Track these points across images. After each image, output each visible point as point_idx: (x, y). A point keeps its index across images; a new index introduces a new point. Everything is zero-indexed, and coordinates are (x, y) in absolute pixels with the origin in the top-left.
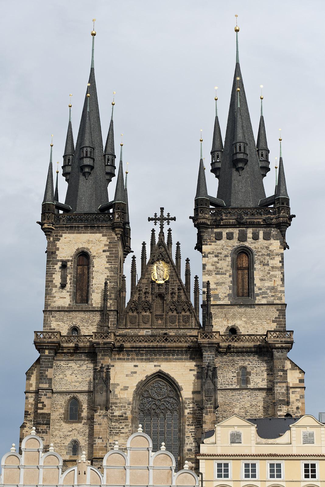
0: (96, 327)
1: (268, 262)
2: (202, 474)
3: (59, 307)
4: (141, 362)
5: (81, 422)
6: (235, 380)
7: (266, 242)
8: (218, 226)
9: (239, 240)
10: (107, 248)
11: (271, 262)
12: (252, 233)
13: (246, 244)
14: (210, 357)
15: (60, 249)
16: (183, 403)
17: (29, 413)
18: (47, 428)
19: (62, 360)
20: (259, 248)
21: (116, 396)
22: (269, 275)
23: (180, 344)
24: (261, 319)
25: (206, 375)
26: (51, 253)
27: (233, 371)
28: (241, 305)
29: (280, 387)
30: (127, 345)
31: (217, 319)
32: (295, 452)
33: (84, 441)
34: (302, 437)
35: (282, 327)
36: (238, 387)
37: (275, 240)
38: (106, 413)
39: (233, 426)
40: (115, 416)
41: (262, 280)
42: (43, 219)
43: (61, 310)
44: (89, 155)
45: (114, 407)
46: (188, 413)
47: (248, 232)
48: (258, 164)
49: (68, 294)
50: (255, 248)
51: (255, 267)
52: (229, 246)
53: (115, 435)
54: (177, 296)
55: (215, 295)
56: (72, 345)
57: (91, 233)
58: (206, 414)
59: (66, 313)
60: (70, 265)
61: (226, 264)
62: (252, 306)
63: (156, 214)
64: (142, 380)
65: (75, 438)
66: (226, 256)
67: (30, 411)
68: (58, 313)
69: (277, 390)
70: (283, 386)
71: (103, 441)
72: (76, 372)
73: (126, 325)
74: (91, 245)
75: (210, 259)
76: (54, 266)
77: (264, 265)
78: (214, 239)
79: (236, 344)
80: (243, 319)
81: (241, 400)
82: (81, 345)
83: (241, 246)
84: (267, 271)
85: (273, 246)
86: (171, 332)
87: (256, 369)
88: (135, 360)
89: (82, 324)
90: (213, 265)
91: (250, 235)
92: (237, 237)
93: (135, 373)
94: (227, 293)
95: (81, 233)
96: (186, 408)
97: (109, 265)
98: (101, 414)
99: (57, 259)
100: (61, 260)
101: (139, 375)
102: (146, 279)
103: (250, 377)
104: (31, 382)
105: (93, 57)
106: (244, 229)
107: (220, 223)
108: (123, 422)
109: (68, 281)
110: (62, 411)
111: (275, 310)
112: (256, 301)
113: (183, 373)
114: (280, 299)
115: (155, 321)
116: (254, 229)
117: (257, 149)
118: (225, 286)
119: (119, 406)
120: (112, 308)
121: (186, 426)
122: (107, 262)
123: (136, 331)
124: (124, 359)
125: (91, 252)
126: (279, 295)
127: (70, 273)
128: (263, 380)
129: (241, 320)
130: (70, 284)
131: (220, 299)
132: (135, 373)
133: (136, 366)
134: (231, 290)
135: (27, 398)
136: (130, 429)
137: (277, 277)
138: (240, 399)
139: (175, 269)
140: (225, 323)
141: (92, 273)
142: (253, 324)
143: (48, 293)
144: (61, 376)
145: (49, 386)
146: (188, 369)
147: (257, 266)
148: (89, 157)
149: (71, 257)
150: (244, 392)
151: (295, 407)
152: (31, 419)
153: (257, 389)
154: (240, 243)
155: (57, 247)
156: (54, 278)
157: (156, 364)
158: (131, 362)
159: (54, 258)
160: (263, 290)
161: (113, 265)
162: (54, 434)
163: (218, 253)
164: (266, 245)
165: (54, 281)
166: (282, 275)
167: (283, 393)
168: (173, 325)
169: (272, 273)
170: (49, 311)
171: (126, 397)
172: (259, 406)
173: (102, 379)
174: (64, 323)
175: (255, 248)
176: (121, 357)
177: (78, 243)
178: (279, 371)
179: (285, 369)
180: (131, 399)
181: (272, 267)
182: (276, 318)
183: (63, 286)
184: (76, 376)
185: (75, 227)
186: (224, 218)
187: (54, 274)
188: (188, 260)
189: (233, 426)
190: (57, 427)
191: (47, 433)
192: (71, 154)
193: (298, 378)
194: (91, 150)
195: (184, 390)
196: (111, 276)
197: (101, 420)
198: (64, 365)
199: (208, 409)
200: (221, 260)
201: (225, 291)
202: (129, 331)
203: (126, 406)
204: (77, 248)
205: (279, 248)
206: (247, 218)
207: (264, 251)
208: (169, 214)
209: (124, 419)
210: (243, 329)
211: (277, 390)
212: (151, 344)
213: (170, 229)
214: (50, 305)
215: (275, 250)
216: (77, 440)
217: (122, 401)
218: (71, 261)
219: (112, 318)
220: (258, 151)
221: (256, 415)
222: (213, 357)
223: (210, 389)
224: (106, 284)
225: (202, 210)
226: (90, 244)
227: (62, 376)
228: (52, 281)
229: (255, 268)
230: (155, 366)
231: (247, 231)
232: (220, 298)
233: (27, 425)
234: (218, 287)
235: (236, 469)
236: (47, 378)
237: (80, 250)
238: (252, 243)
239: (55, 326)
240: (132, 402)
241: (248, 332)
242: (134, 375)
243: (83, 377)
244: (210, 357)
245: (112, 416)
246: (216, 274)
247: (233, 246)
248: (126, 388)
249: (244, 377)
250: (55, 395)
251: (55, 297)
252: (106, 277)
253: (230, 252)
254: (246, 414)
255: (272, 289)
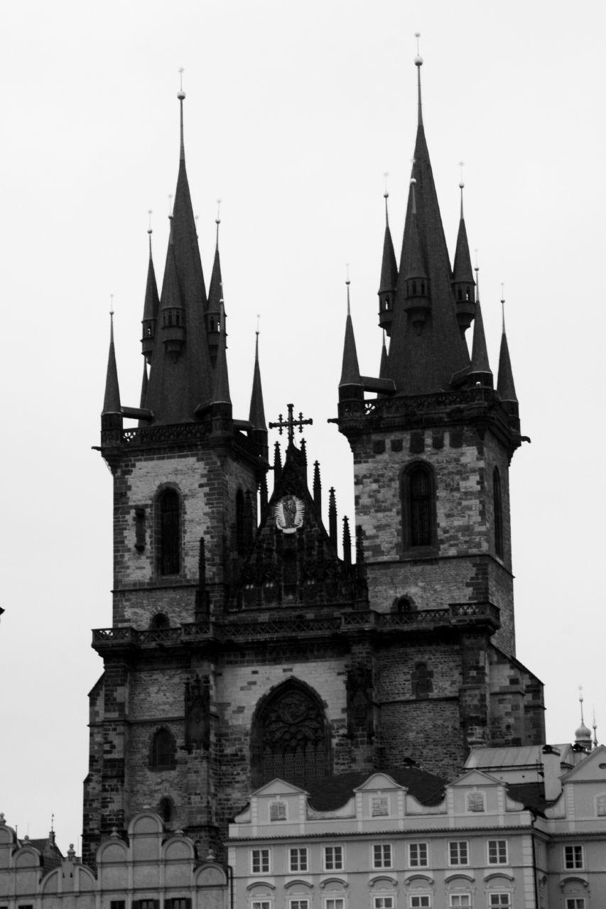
0: (192, 612)
1: (458, 484)
2: (231, 868)
3: (135, 584)
4: (263, 665)
5: (174, 769)
6: (408, 685)
7: (454, 450)
8: (378, 430)
9: (411, 451)
10: (204, 480)
11: (463, 484)
12: (433, 437)
13: (424, 457)
14: (362, 653)
15: (133, 488)
16: (331, 727)
17: (96, 758)
18: (118, 782)
19: (144, 671)
20: (443, 462)
21: (226, 722)
22: (459, 508)
23: (320, 633)
24: (449, 583)
25: (357, 684)
26: (120, 496)
27: (405, 671)
28: (415, 562)
29: (470, 696)
30: (240, 639)
31: (380, 588)
32: (360, 828)
33: (180, 798)
34: (371, 805)
35: (481, 593)
36: (413, 698)
37: (469, 446)
38: (205, 753)
39: (274, 795)
40: (226, 756)
41: (448, 516)
42: (103, 440)
43: (139, 588)
44: (174, 322)
45: (224, 742)
46: (337, 745)
47: (426, 436)
48: (453, 310)
49: (148, 561)
50: (438, 463)
51: (438, 494)
52: (396, 463)
53: (227, 786)
54: (315, 553)
55: (375, 546)
56: (153, 645)
57: (180, 457)
58: (356, 747)
59: (147, 593)
60: (150, 514)
61: (390, 494)
62: (434, 562)
63: (281, 416)
64: (264, 695)
65: (166, 794)
66: (391, 480)
67: (97, 756)
68: (134, 593)
69: (466, 701)
70: (476, 695)
71: (201, 798)
72: (164, 688)
73: (239, 605)
74: (180, 477)
75: (366, 487)
76: (124, 517)
77: (452, 490)
78: (372, 453)
79: (406, 628)
80: (420, 584)
81: (418, 718)
82: (168, 643)
83: (414, 460)
84: (457, 501)
85: (466, 458)
86: (308, 613)
87: (440, 666)
88: (253, 662)
89: (171, 610)
90: (370, 496)
91: (429, 441)
92: (408, 446)
93: (254, 683)
94: (394, 542)
95: (163, 458)
96: (334, 737)
97: (210, 508)
98: (197, 755)
99: (130, 504)
100: (135, 506)
101: (260, 686)
102: (268, 526)
103: (432, 680)
104: (96, 709)
105: (182, 139)
106: (420, 431)
107: (379, 425)
108: (238, 765)
109: (148, 540)
110: (146, 752)
111: (470, 565)
112: (440, 552)
113: (324, 679)
114: (479, 545)
115: (283, 597)
116: (435, 429)
117: (452, 282)
118: (390, 530)
119: (231, 740)
120: (217, 580)
121: (335, 766)
122: (206, 504)
123: (255, 615)
124: (237, 663)
125: (180, 490)
126: (477, 540)
127: (150, 527)
128: (453, 683)
129: (417, 585)
130: (151, 544)
131: (382, 553)
132: (254, 683)
133: (255, 672)
134: (400, 538)
135: (91, 735)
136: (249, 775)
137: (474, 509)
138: (418, 716)
139: (313, 507)
140: (391, 592)
141: (184, 524)
142: (435, 591)
143: (118, 564)
144: (142, 696)
145: (119, 715)
146: (335, 672)
147: (441, 493)
148: (184, 318)
149: (150, 499)
150: (423, 705)
151: (505, 725)
152: (99, 767)
153: (444, 698)
154: (413, 455)
155: (129, 484)
156: (126, 537)
157: (285, 666)
158: (247, 666)
159: (125, 503)
160: (451, 534)
161: (215, 507)
162: (135, 789)
163: (379, 476)
164: (455, 456)
165: (126, 542)
166: (481, 506)
167: (475, 706)
168: (312, 601)
169: (464, 503)
170: (120, 591)
171: (240, 723)
172: (448, 727)
173: (198, 700)
174: (145, 610)
175: (438, 463)
176: (232, 658)
177: (160, 475)
178: (470, 669)
179: (481, 664)
180: (249, 726)
181: (466, 493)
182: (472, 579)
183: (140, 548)
184: (165, 695)
185: (155, 449)
186: (385, 416)
187: (125, 529)
188: (332, 491)
189: (274, 795)
190: (139, 779)
191: (117, 790)
192: (152, 318)
193: (508, 676)
194: (178, 312)
195: (330, 706)
196: (212, 527)
197: (197, 765)
198: (146, 678)
199: (359, 739)
200: (383, 487)
201: (391, 539)
202: (243, 615)
203: (243, 739)
204: (158, 485)
205: (475, 459)
206: (422, 413)
207: (451, 467)
208: (301, 414)
209: (239, 760)
210: (420, 601)
211: (466, 701)
212: (275, 635)
213: (303, 439)
214: (121, 582)
215: (469, 463)
216: (170, 797)
217: (234, 729)
218: (151, 506)
219: (216, 596)
220: (453, 285)
221: (443, 742)
222: (367, 653)
223: (361, 705)
224: (202, 541)
225: (348, 405)
226: (179, 476)
227: (143, 695)
228: (123, 542)
229: (438, 497)
230: (285, 670)
231: (423, 435)
232: (383, 551)
233: (93, 778)
234: (380, 533)
235: (280, 860)
236: (116, 704)
237: (164, 487)
238: (432, 454)
239: (130, 615)
240: (250, 732)
241: (427, 605)
242: (253, 687)
243: (175, 696)
244: (362, 653)
245: (221, 756)
246: (376, 511)
247: (403, 462)
248: (241, 710)
249: (423, 681)
250: (134, 727)
251: (128, 568)
252: (205, 529)
253: (398, 472)
254: (427, 741)
255: (466, 531)
